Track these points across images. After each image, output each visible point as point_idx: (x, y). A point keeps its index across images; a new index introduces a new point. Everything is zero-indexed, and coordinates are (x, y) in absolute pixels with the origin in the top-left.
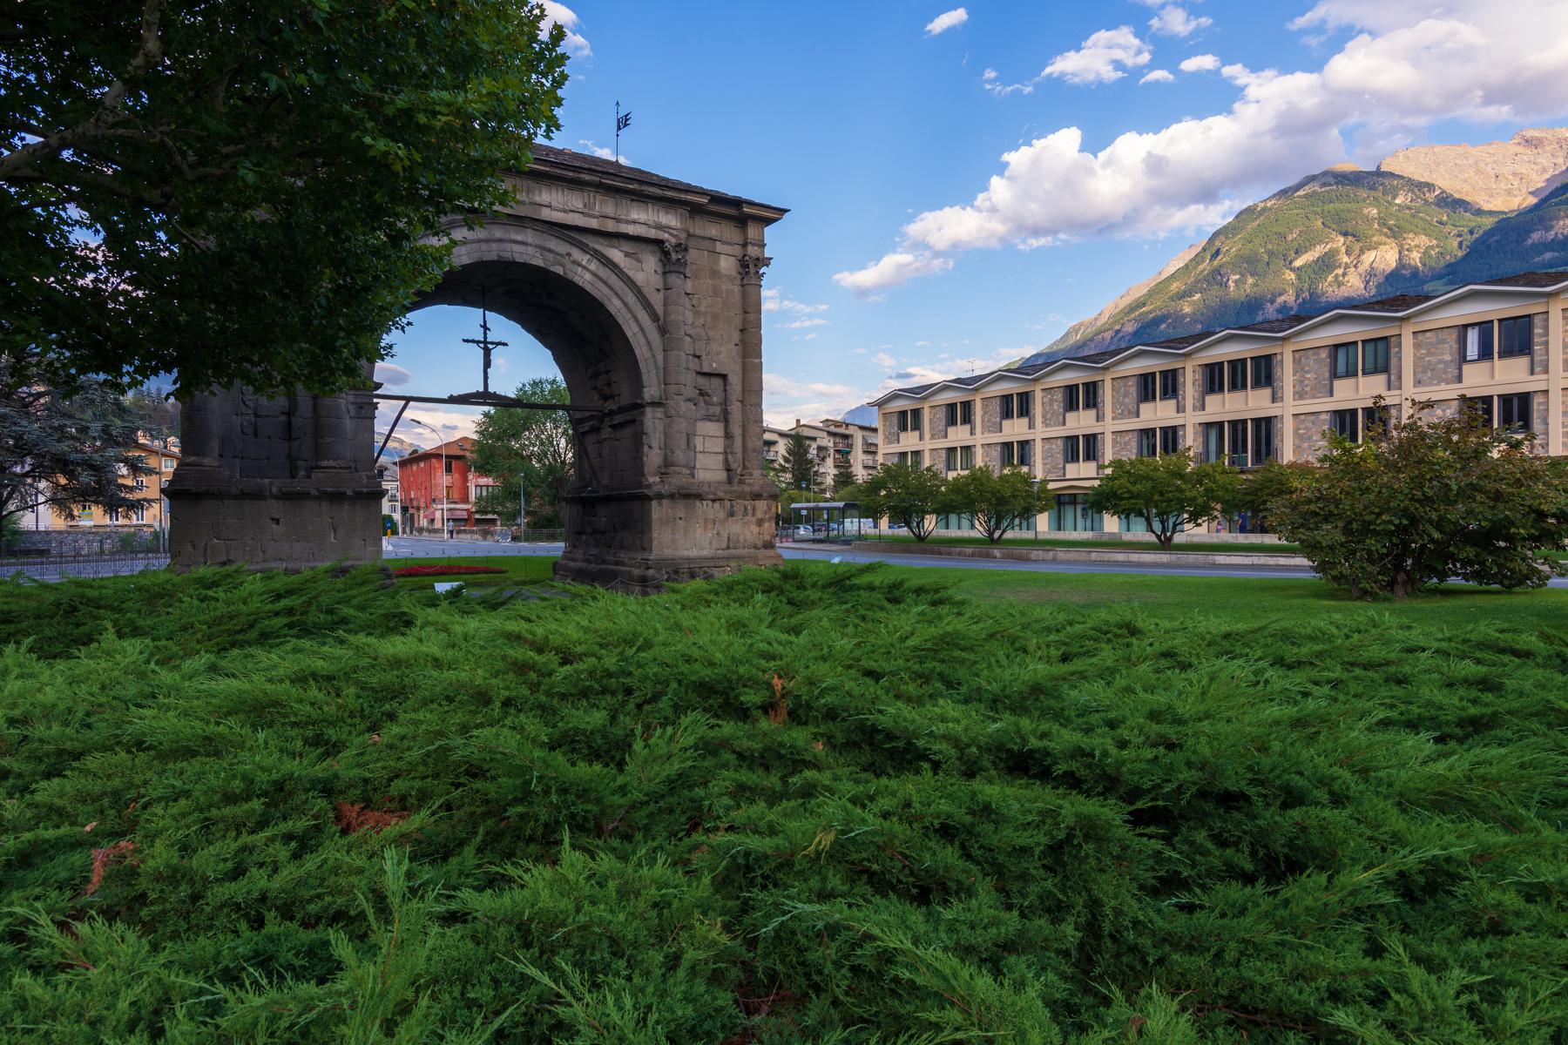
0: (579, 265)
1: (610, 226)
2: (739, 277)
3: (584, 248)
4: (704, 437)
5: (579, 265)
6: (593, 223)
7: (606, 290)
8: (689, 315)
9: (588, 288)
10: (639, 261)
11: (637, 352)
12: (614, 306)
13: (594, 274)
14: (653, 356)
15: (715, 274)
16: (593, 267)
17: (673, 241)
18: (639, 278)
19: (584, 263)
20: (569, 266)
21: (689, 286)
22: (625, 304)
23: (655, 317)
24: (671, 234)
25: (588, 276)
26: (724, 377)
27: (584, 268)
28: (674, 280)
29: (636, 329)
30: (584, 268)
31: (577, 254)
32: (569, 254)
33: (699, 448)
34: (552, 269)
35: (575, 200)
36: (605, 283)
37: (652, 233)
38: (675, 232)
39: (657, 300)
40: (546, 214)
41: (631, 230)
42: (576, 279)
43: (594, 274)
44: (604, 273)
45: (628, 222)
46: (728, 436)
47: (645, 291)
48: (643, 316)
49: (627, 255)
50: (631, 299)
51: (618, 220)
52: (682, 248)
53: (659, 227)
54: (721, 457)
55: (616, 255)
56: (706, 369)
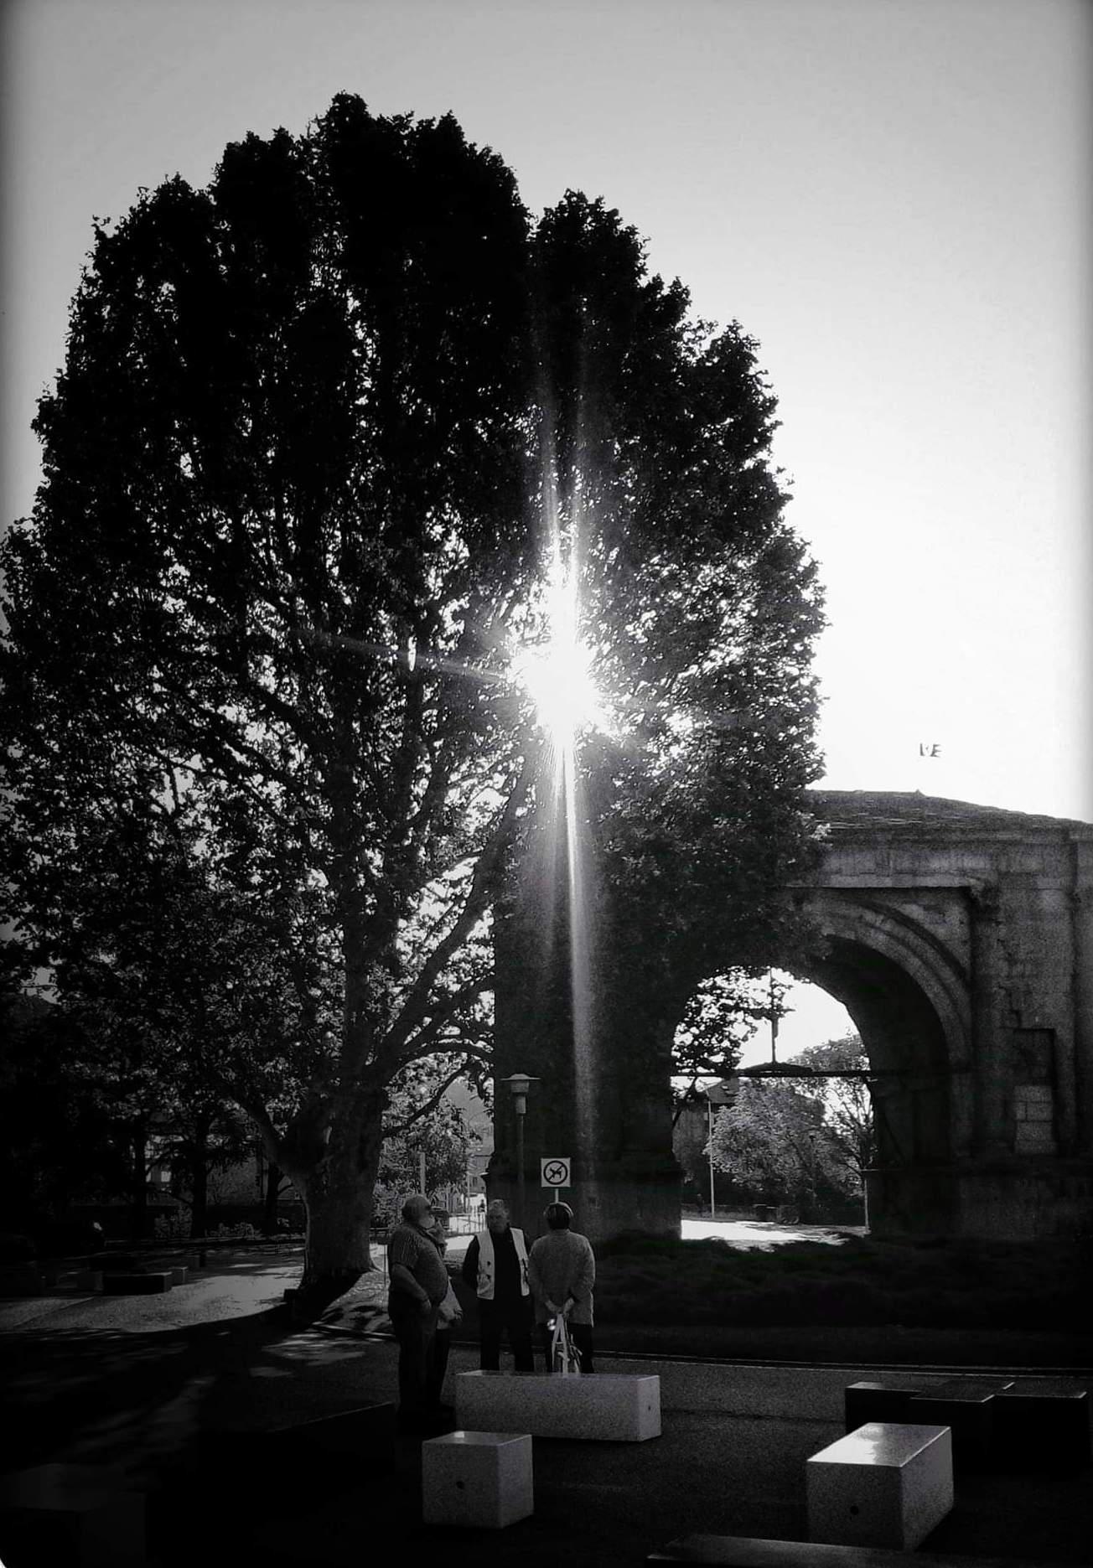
0: (873, 926)
1: (907, 882)
2: (1067, 913)
3: (876, 910)
4: (1026, 1104)
5: (873, 926)
6: (888, 882)
7: (904, 951)
8: (1003, 966)
9: (882, 949)
10: (941, 912)
11: (941, 1013)
12: (913, 964)
13: (889, 934)
14: (960, 1016)
15: (1036, 915)
16: (888, 927)
17: (980, 886)
18: (941, 932)
19: (878, 924)
20: (861, 931)
21: (1003, 931)
22: (925, 962)
23: (959, 971)
24: (978, 879)
25: (882, 937)
26: (1051, 1033)
27: (878, 929)
28: (984, 930)
29: (937, 988)
30: (878, 929)
31: (869, 916)
32: (861, 917)
33: (1020, 1114)
34: (842, 935)
35: (867, 861)
36: (902, 942)
37: (956, 882)
38: (983, 877)
39: (962, 953)
40: (837, 881)
41: (930, 882)
42: (870, 942)
43: (889, 934)
44: (900, 931)
45: (926, 874)
46: (1058, 1103)
47: (950, 946)
48: (947, 974)
49: (927, 908)
50: (931, 954)
51: (914, 873)
52: (991, 891)
53: (963, 873)
54: (1048, 1127)
55: (914, 911)
56: (1025, 1025)
